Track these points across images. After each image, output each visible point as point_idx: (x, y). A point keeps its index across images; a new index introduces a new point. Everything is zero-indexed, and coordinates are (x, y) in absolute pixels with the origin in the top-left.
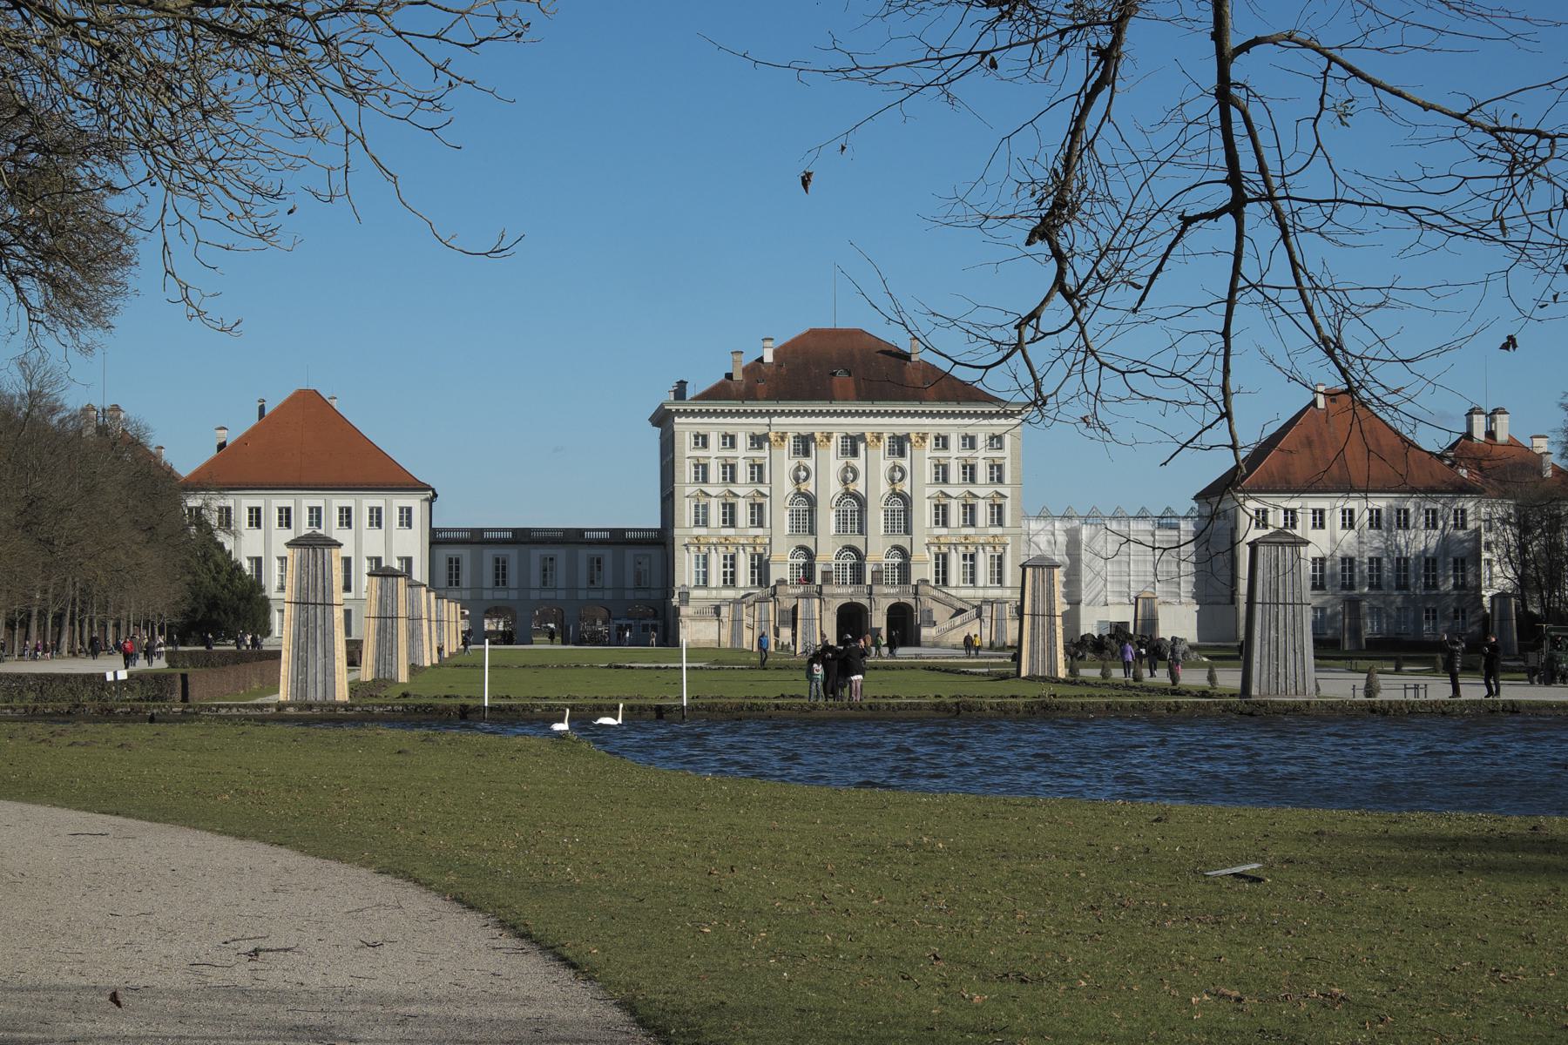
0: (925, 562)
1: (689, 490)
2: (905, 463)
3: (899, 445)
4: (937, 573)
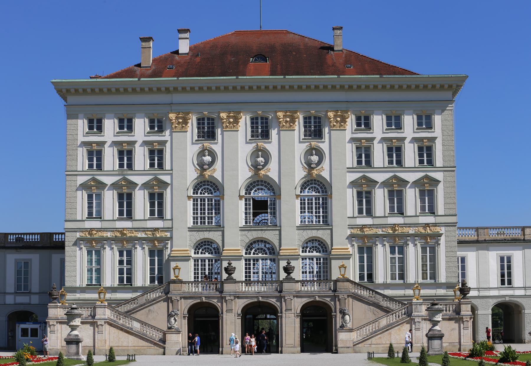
0: (347, 257)
1: (81, 180)
2: (324, 146)
4: (362, 268)
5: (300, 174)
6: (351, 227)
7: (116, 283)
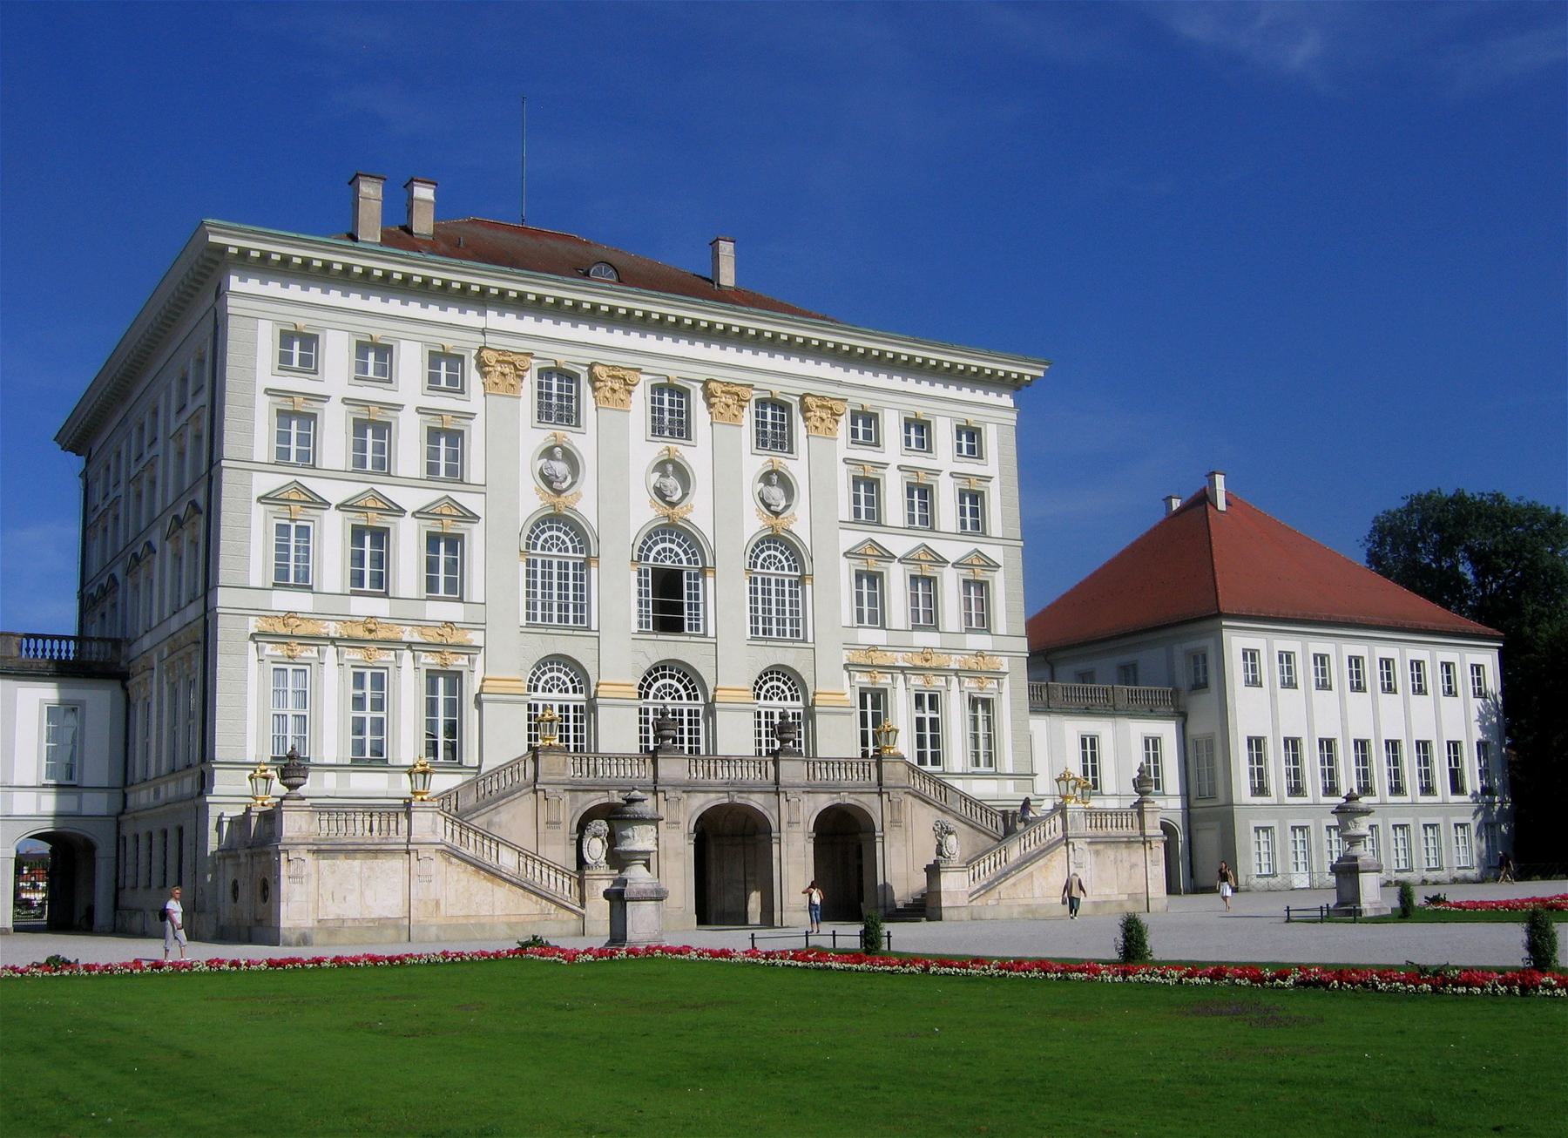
1: (266, 483)
2: (796, 468)
3: (775, 427)
5: (753, 524)
6: (851, 646)
7: (348, 757)
